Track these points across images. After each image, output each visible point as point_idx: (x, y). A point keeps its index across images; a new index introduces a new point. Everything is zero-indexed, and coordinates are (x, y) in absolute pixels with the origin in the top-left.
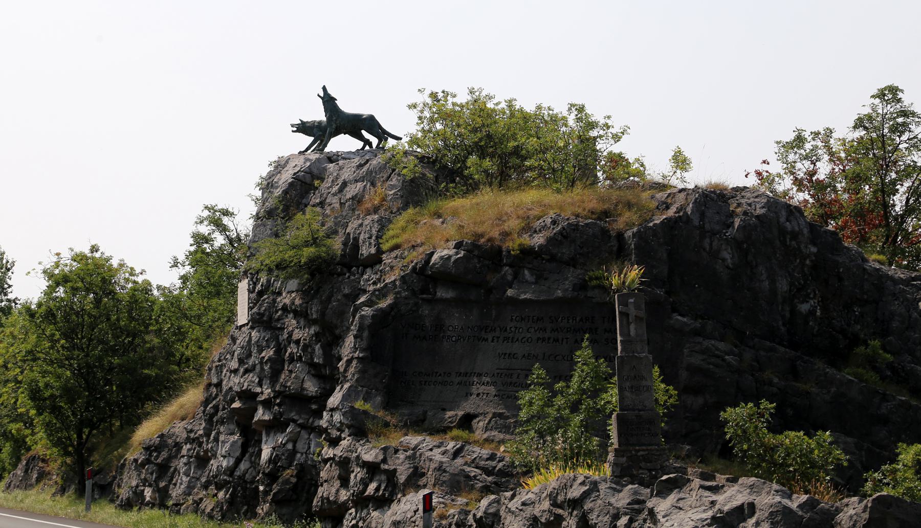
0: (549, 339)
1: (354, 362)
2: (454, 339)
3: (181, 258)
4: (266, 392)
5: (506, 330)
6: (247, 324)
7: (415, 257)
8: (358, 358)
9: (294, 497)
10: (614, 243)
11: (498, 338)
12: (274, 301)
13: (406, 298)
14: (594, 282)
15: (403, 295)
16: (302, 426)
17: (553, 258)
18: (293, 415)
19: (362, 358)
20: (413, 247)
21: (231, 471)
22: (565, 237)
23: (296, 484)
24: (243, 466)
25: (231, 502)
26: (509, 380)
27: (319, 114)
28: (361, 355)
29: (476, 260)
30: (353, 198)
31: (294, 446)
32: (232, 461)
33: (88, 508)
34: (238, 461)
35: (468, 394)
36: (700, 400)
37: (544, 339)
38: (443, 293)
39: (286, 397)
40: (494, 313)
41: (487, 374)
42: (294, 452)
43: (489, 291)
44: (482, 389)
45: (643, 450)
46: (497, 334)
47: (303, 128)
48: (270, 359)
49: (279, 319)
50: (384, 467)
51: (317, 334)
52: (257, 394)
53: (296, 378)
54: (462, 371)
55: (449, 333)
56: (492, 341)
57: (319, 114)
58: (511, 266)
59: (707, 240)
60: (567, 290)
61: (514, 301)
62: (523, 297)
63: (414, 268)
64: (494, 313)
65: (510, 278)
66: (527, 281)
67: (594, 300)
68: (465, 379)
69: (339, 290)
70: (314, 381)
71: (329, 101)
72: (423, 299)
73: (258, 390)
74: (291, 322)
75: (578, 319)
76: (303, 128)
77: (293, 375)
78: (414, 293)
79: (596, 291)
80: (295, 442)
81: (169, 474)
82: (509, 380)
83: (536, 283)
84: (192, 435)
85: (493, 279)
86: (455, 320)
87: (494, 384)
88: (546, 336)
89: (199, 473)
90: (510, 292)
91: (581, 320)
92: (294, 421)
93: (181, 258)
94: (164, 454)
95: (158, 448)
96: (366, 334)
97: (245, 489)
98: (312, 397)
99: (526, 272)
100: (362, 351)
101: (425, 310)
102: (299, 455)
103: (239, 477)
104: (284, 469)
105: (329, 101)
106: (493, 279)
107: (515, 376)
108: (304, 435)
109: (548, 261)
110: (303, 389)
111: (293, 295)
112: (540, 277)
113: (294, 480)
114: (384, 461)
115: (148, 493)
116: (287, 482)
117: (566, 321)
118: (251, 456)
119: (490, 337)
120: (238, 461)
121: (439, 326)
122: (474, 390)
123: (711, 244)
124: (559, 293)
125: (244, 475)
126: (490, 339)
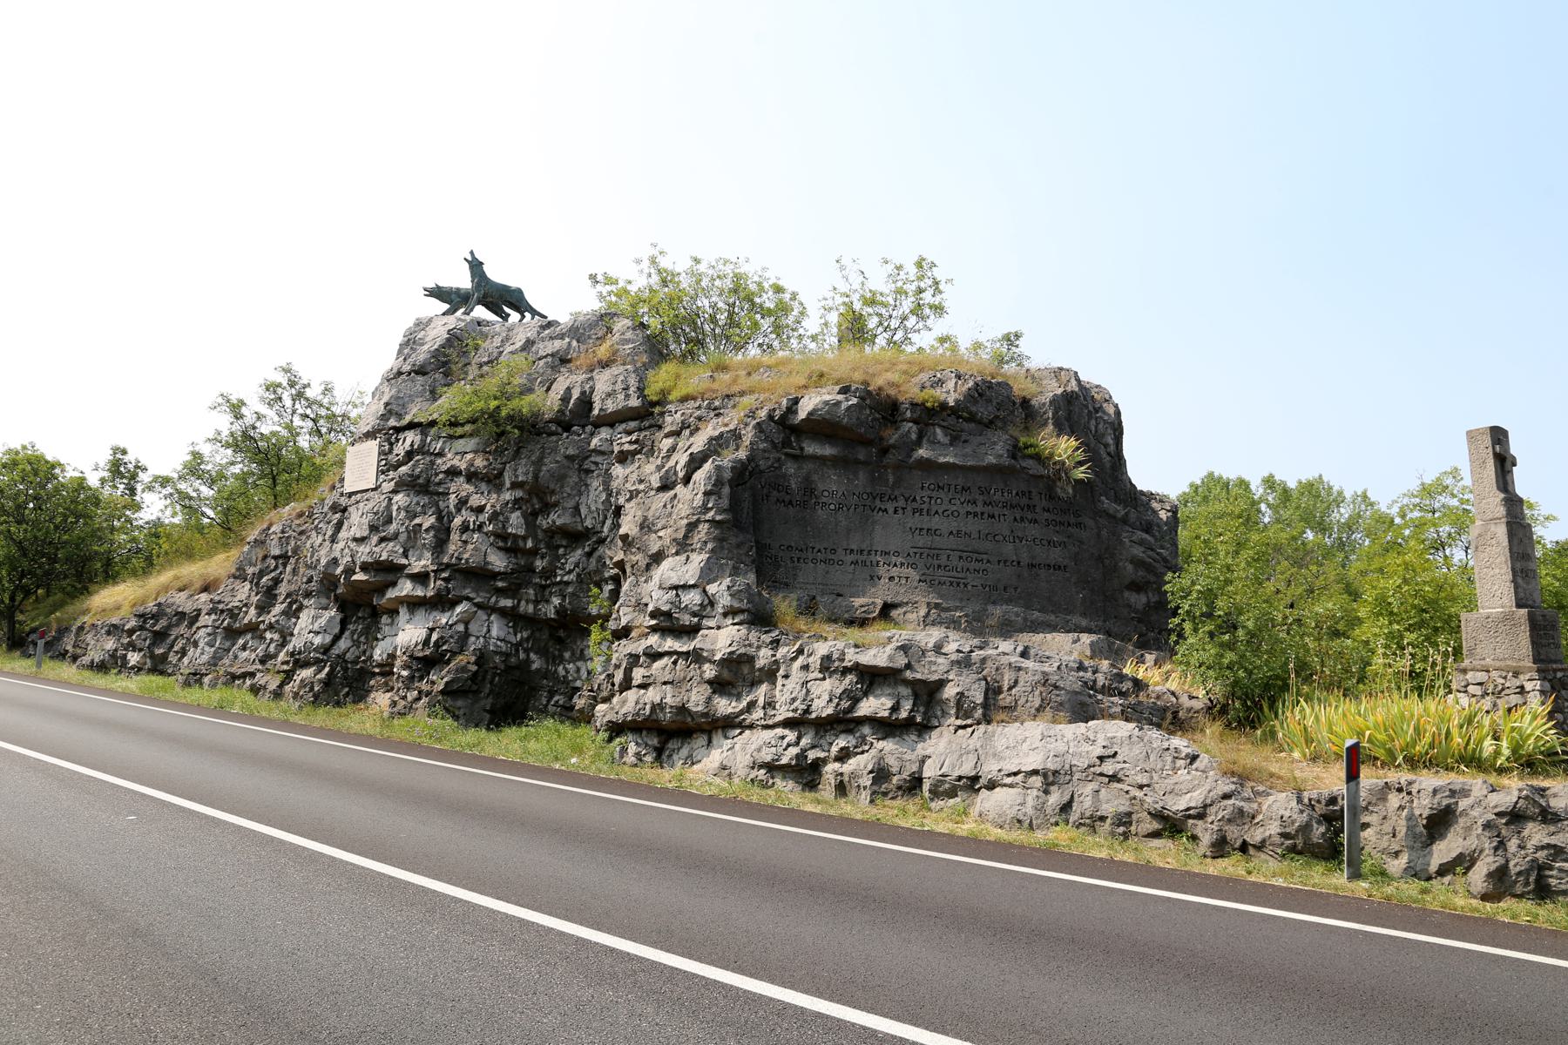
1: (703, 528)
3: (102, 465)
4: (421, 562)
7: (767, 403)
8: (712, 521)
9: (475, 688)
10: (1019, 412)
12: (432, 463)
13: (764, 451)
14: (1031, 451)
16: (479, 606)
17: (972, 418)
18: (467, 592)
21: (326, 649)
22: (980, 395)
23: (475, 673)
24: (343, 644)
25: (328, 683)
26: (936, 562)
27: (463, 281)
28: (718, 518)
30: (552, 355)
31: (466, 628)
32: (328, 639)
33: (39, 665)
34: (337, 638)
35: (874, 578)
36: (1143, 599)
37: (976, 514)
38: (811, 448)
39: (461, 571)
40: (891, 479)
41: (897, 554)
42: (466, 635)
43: (885, 451)
44: (895, 571)
46: (901, 503)
47: (438, 293)
48: (432, 527)
49: (439, 484)
50: (908, 674)
51: (516, 501)
52: (404, 567)
53: (476, 549)
54: (854, 547)
57: (463, 281)
58: (915, 422)
59: (1093, 422)
61: (927, 466)
62: (942, 460)
63: (770, 417)
64: (891, 479)
65: (914, 436)
68: (861, 558)
69: (555, 450)
70: (501, 554)
71: (476, 266)
72: (787, 454)
73: (404, 561)
74: (460, 487)
76: (438, 293)
77: (470, 547)
79: (1031, 462)
80: (467, 624)
81: (169, 641)
82: (936, 562)
84: (221, 606)
85: (892, 437)
86: (832, 484)
87: (913, 566)
88: (978, 510)
89: (228, 644)
90: (922, 452)
92: (468, 599)
93: (102, 465)
94: (163, 623)
95: (156, 617)
96: (726, 490)
97: (346, 669)
98: (499, 573)
99: (938, 431)
100: (720, 511)
101: (790, 468)
102: (472, 639)
103: (338, 656)
104: (454, 654)
105: (476, 266)
106: (892, 437)
108: (482, 615)
109: (965, 420)
110: (487, 563)
111: (469, 456)
112: (954, 440)
113: (474, 668)
114: (909, 666)
115: (134, 658)
116: (464, 669)
118: (353, 633)
119: (890, 507)
120: (337, 638)
121: (809, 490)
122: (882, 570)
124: (991, 459)
125: (345, 654)
126: (891, 511)
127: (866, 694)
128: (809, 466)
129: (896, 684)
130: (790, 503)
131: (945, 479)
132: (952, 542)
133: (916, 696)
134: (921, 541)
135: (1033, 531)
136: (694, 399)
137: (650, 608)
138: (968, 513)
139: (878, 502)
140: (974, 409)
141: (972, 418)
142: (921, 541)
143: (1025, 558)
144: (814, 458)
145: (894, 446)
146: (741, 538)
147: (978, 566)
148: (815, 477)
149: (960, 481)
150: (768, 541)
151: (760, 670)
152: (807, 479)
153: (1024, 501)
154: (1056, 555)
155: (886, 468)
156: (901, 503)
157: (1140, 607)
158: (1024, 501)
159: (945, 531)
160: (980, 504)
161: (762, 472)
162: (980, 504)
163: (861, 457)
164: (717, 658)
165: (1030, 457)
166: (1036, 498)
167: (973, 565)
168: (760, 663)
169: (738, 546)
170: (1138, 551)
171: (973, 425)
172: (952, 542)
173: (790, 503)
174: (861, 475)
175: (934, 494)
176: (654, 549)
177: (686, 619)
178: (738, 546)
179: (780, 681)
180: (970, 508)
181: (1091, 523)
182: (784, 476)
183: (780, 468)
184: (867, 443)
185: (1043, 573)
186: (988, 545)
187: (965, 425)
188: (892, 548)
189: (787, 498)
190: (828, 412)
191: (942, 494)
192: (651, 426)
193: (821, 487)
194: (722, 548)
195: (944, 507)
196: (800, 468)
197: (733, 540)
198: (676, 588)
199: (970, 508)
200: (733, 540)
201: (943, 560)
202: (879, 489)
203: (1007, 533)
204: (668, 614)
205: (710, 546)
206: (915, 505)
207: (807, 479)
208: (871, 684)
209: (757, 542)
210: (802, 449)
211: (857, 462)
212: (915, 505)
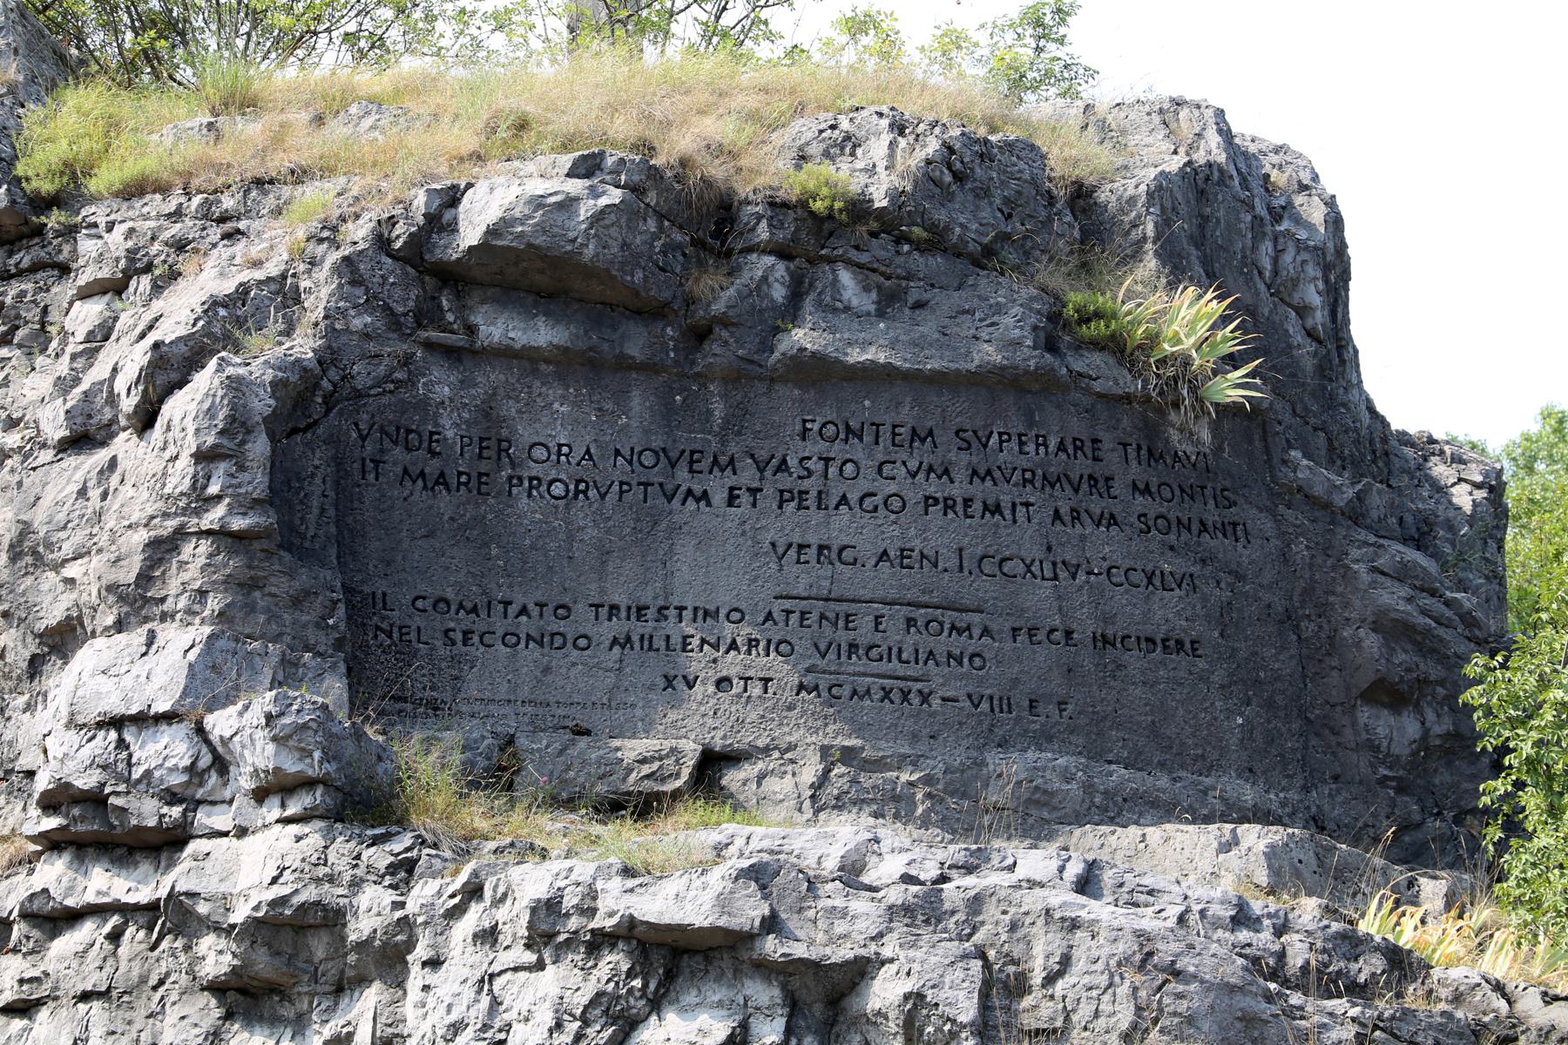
0: (967, 502)
1: (196, 553)
2: (558, 489)
5: (783, 466)
6: (750, 250)
8: (219, 534)
11: (753, 491)
13: (367, 336)
14: (1097, 329)
15: (357, 323)
17: (937, 242)
19: (239, 536)
20: (259, 182)
22: (959, 177)
26: (843, 637)
28: (238, 524)
29: (652, 225)
35: (675, 683)
37: (949, 505)
38: (497, 327)
40: (718, 409)
41: (737, 614)
43: (700, 335)
44: (732, 664)
46: (747, 475)
50: (772, 947)
55: (536, 469)
56: (732, 500)
58: (783, 253)
59: (1267, 247)
60: (1017, 344)
61: (815, 372)
62: (856, 356)
63: (381, 241)
64: (718, 409)
65: (779, 293)
66: (847, 309)
67: (1097, 386)
68: (637, 629)
72: (429, 346)
75: (1053, 443)
78: (394, 322)
82: (843, 637)
83: (881, 314)
85: (720, 294)
86: (555, 424)
87: (781, 647)
88: (957, 491)
90: (803, 337)
91: (1061, 447)
96: (259, 447)
99: (845, 277)
100: (244, 505)
101: (440, 383)
106: (720, 294)
107: (865, 624)
112: (889, 302)
114: (771, 924)
117: (1014, 445)
121: (493, 443)
123: (1275, 261)
124: (988, 353)
126: (719, 497)
127: (656, 1005)
128: (490, 377)
129: (738, 973)
130: (442, 479)
131: (866, 409)
132: (886, 581)
133: (794, 1006)
134: (802, 579)
135: (1106, 546)
136: (163, 189)
137: (42, 783)
138: (930, 501)
139: (682, 474)
140: (941, 216)
141: (937, 242)
142: (802, 579)
143: (1086, 625)
144: (506, 354)
145: (724, 321)
146: (304, 579)
147: (957, 643)
148: (510, 409)
149: (907, 415)
150: (381, 586)
151: (361, 946)
152: (487, 412)
153: (1081, 466)
154: (1168, 612)
155: (703, 379)
156: (747, 475)
157: (1401, 749)
158: (1081, 466)
159: (867, 551)
160: (960, 475)
161: (359, 394)
162: (960, 475)
163: (635, 349)
164: (238, 916)
165: (1096, 345)
166: (1112, 459)
167: (945, 643)
168: (361, 927)
169: (296, 602)
170: (1393, 597)
171: (937, 261)
172: (886, 581)
173: (442, 479)
174: (637, 401)
175: (837, 450)
176: (53, 613)
177: (148, 812)
178: (296, 602)
179: (417, 977)
180: (934, 487)
181: (1261, 523)
182: (423, 405)
183: (411, 382)
184: (651, 313)
185: (1134, 660)
186: (984, 588)
187: (919, 262)
188: (724, 600)
189: (432, 467)
190: (541, 228)
191: (857, 450)
192: (35, 268)
193: (525, 433)
194: (251, 608)
195: (864, 485)
196: (465, 383)
197: (281, 586)
198: (117, 723)
199: (934, 487)
200: (281, 586)
201: (864, 631)
202: (687, 439)
203: (1038, 554)
204: (95, 800)
205: (214, 603)
206: (785, 481)
207: (487, 412)
208: (670, 977)
209: (347, 589)
210: (471, 330)
211: (625, 365)
212: (785, 481)
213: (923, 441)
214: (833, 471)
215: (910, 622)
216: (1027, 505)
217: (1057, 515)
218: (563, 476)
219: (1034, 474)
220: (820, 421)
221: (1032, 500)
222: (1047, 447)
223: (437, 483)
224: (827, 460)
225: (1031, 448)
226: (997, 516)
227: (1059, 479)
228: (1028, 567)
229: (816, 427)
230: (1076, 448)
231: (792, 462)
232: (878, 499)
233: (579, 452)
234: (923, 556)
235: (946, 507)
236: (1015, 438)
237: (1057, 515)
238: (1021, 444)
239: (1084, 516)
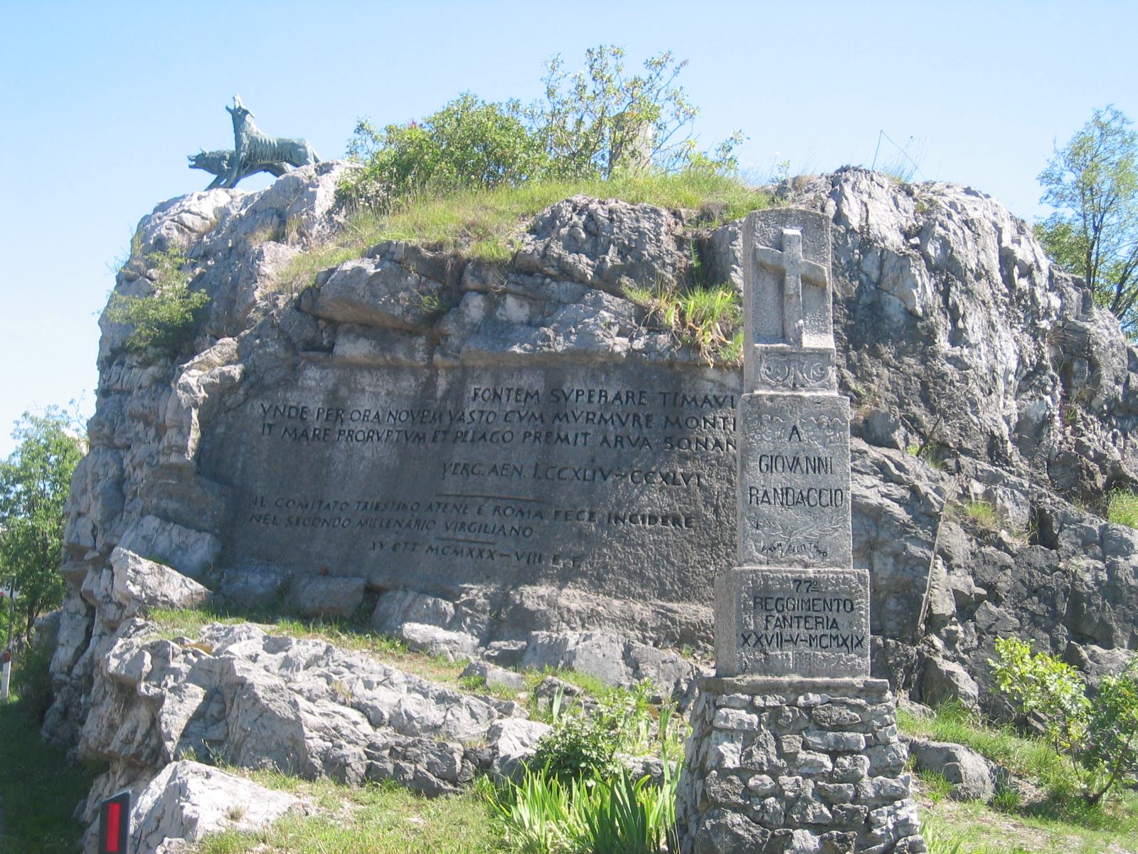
45: (816, 689)
55: (352, 426)
91: (618, 397)
201: (470, 517)
213: (532, 397)
214: (484, 418)
215: (496, 509)
216: (586, 434)
217: (605, 440)
218: (364, 429)
219: (594, 415)
220: (483, 389)
221: (589, 431)
222: (606, 398)
223: (302, 435)
224: (482, 412)
225: (596, 399)
226: (565, 442)
227: (612, 417)
228: (576, 473)
229: (480, 393)
230: (628, 397)
231: (467, 414)
232: (500, 436)
233: (373, 413)
234: (515, 468)
235: (535, 437)
236: (586, 394)
237: (605, 440)
238: (590, 396)
239: (626, 442)
